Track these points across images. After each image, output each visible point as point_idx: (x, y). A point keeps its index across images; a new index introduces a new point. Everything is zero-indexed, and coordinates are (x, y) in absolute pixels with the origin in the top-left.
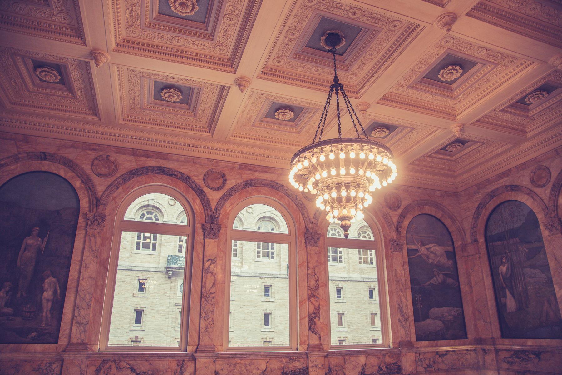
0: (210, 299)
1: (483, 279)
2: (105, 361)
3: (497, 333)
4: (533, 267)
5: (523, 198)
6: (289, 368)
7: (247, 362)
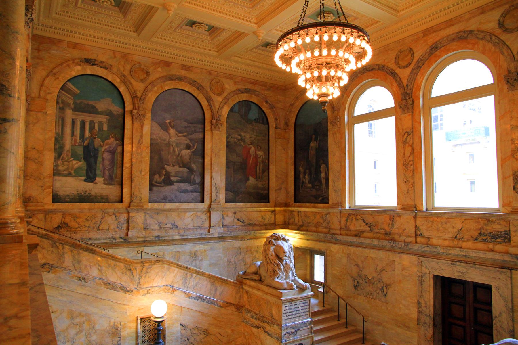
0: (409, 166)
2: (350, 214)
6: (487, 230)
7: (443, 221)
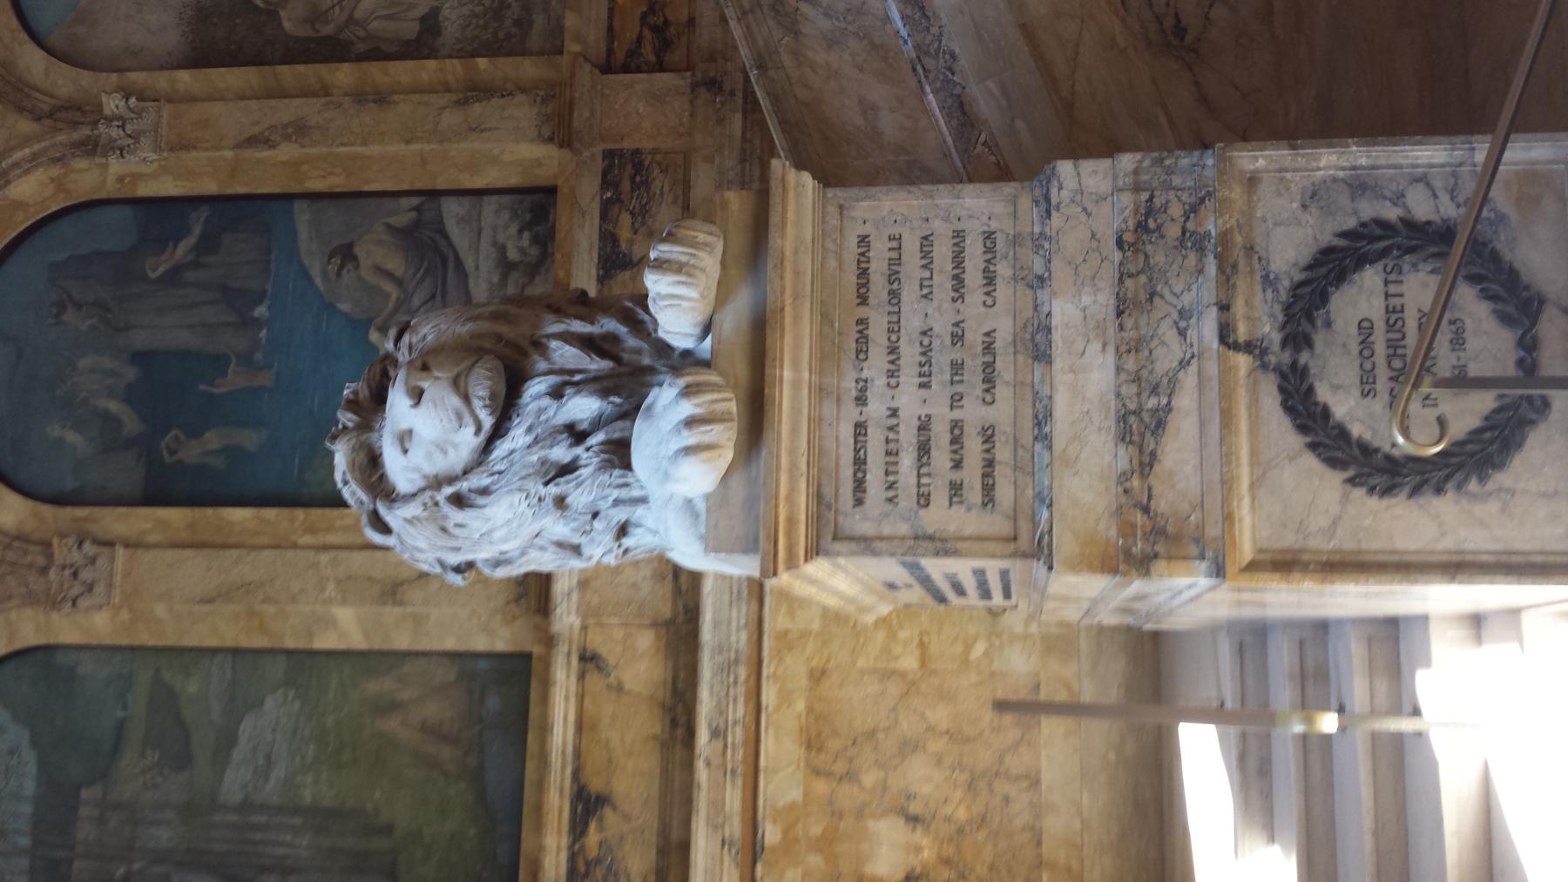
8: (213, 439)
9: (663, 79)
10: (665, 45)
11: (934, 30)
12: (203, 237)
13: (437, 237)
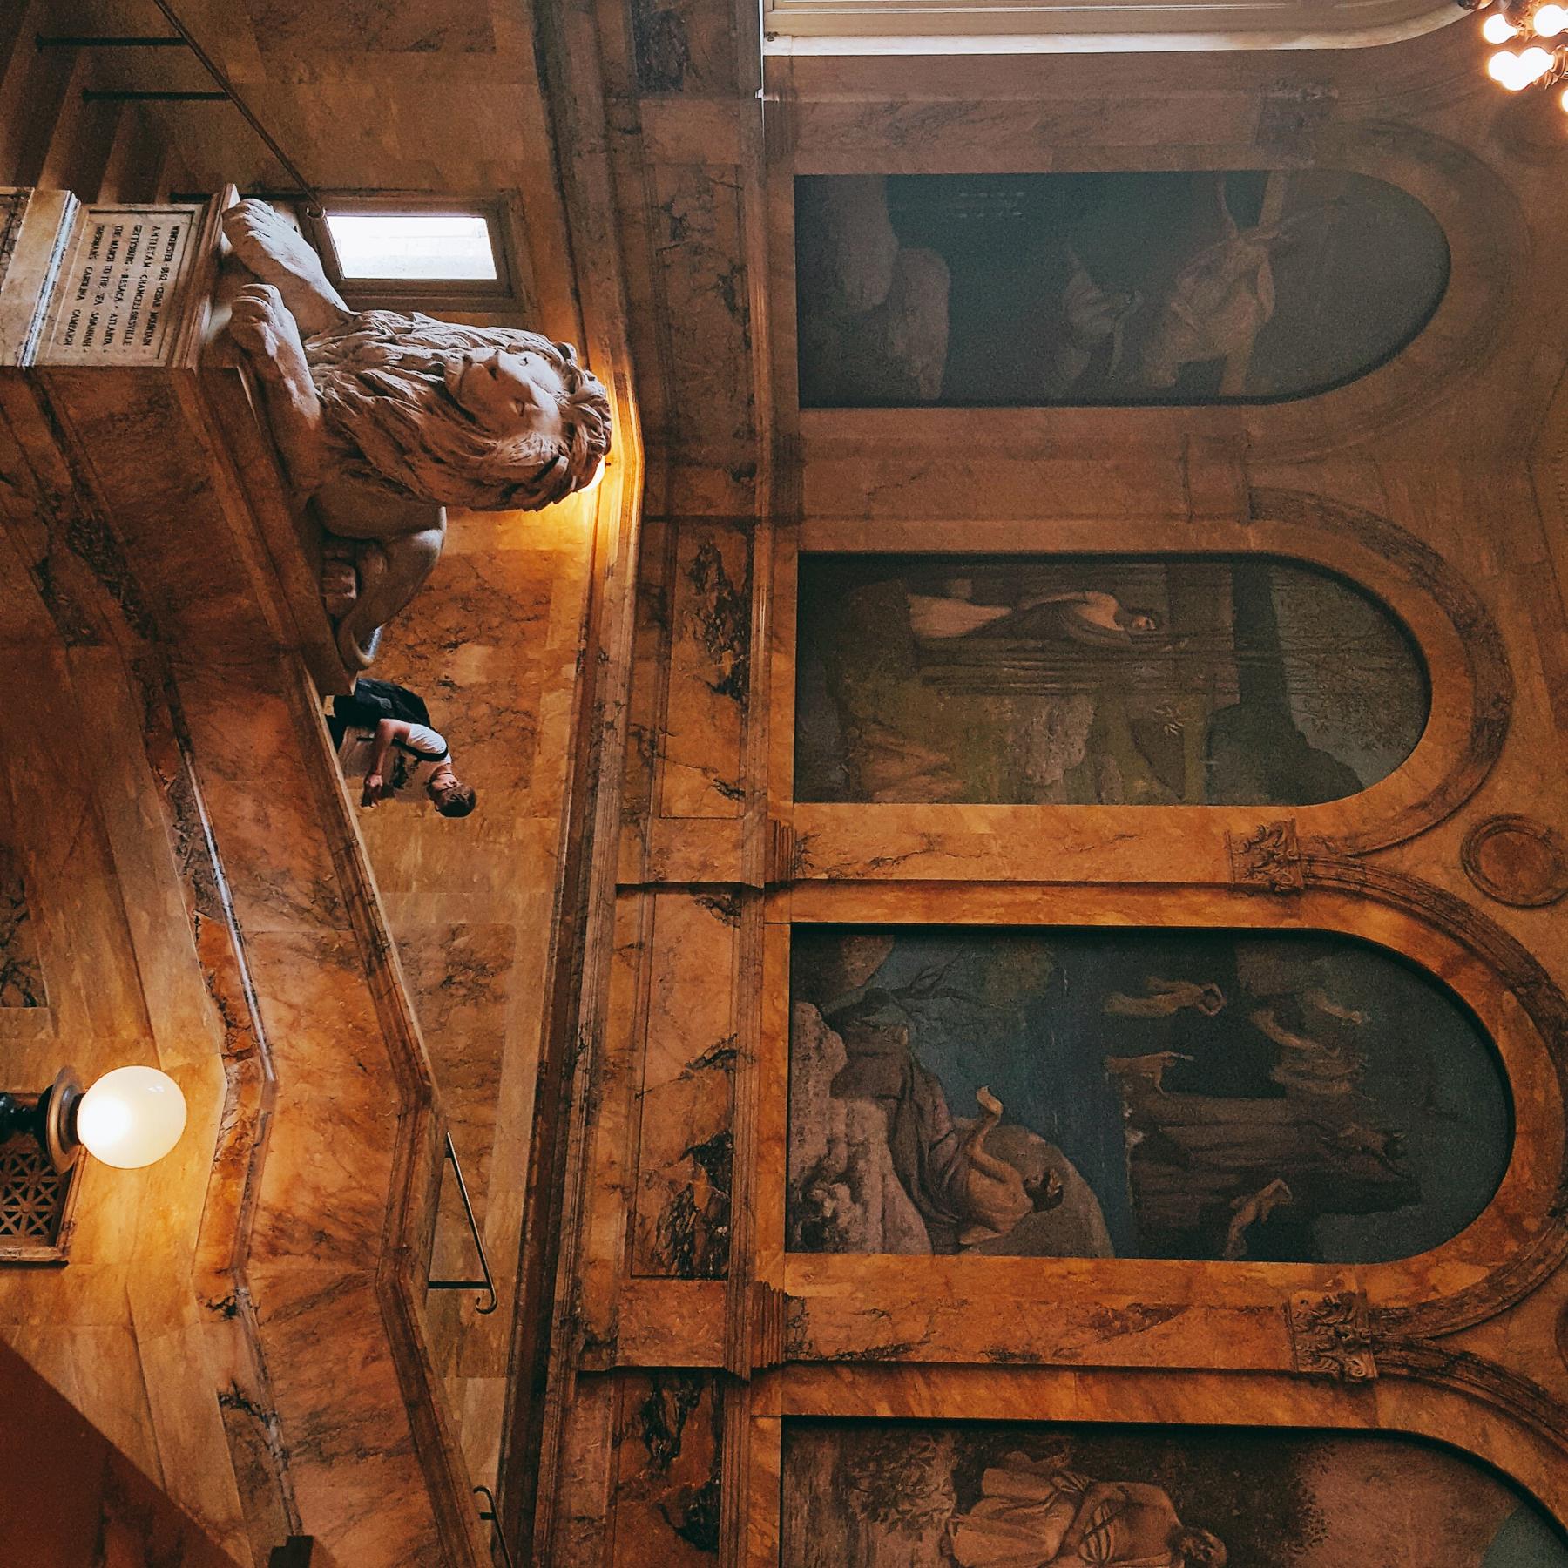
1: (1070, 516)
3: (820, 540)
4: (1097, 740)
5: (1429, 763)
8: (1164, 1004)
9: (650, 1358)
10: (650, 1412)
11: (190, 871)
12: (1225, 1227)
13: (933, 1213)
